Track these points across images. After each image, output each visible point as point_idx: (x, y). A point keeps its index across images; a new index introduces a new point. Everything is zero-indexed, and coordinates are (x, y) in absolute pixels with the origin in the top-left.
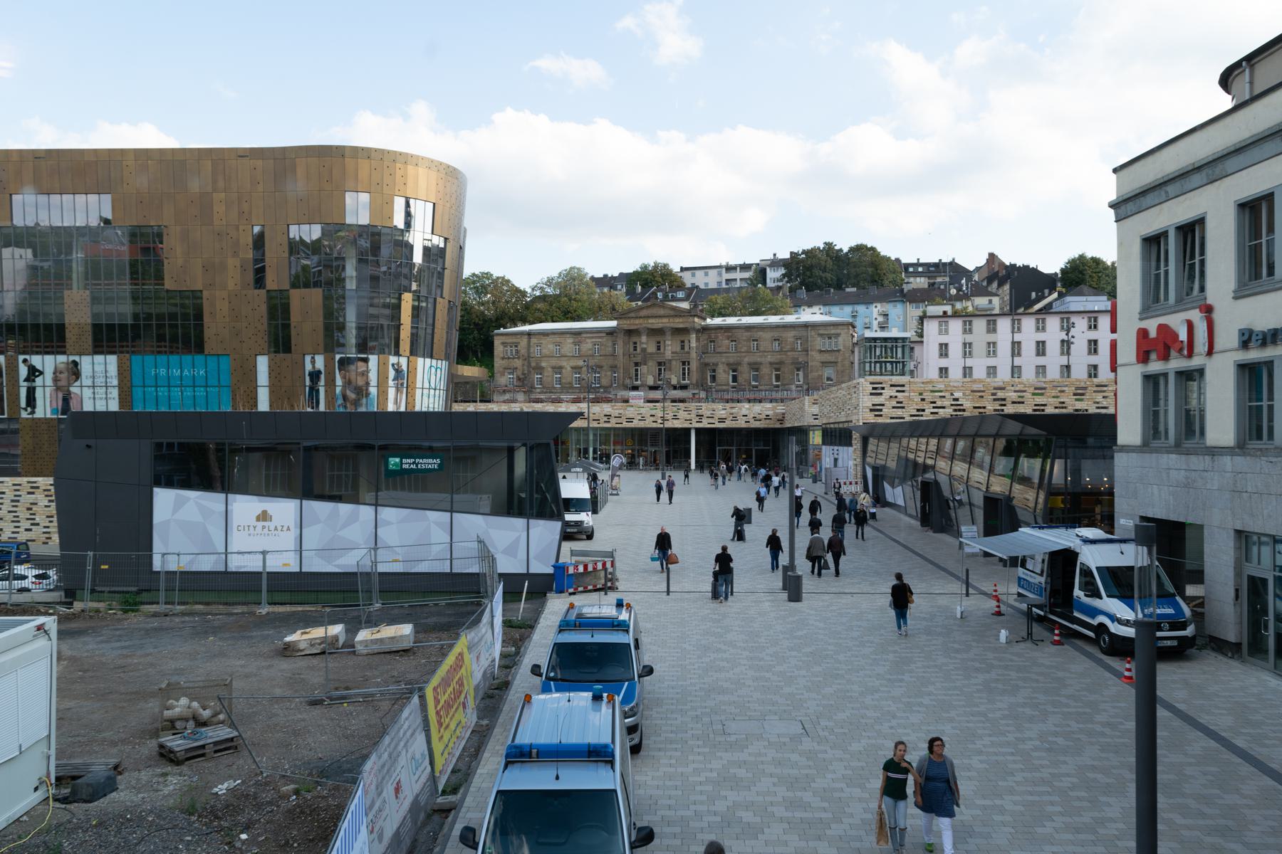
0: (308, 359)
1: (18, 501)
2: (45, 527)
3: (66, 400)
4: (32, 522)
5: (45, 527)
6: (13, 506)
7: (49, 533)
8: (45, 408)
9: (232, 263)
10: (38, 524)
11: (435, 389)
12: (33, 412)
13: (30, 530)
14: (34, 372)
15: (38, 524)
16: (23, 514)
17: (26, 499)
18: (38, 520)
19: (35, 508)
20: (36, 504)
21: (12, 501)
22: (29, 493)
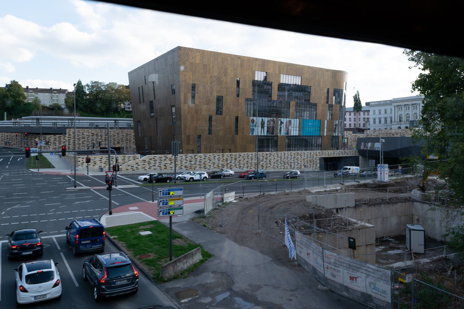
0: (335, 121)
3: (288, 131)
8: (283, 133)
9: (323, 97)
12: (280, 134)
14: (282, 123)
15: (299, 164)
16: (296, 161)
19: (298, 159)
21: (294, 158)
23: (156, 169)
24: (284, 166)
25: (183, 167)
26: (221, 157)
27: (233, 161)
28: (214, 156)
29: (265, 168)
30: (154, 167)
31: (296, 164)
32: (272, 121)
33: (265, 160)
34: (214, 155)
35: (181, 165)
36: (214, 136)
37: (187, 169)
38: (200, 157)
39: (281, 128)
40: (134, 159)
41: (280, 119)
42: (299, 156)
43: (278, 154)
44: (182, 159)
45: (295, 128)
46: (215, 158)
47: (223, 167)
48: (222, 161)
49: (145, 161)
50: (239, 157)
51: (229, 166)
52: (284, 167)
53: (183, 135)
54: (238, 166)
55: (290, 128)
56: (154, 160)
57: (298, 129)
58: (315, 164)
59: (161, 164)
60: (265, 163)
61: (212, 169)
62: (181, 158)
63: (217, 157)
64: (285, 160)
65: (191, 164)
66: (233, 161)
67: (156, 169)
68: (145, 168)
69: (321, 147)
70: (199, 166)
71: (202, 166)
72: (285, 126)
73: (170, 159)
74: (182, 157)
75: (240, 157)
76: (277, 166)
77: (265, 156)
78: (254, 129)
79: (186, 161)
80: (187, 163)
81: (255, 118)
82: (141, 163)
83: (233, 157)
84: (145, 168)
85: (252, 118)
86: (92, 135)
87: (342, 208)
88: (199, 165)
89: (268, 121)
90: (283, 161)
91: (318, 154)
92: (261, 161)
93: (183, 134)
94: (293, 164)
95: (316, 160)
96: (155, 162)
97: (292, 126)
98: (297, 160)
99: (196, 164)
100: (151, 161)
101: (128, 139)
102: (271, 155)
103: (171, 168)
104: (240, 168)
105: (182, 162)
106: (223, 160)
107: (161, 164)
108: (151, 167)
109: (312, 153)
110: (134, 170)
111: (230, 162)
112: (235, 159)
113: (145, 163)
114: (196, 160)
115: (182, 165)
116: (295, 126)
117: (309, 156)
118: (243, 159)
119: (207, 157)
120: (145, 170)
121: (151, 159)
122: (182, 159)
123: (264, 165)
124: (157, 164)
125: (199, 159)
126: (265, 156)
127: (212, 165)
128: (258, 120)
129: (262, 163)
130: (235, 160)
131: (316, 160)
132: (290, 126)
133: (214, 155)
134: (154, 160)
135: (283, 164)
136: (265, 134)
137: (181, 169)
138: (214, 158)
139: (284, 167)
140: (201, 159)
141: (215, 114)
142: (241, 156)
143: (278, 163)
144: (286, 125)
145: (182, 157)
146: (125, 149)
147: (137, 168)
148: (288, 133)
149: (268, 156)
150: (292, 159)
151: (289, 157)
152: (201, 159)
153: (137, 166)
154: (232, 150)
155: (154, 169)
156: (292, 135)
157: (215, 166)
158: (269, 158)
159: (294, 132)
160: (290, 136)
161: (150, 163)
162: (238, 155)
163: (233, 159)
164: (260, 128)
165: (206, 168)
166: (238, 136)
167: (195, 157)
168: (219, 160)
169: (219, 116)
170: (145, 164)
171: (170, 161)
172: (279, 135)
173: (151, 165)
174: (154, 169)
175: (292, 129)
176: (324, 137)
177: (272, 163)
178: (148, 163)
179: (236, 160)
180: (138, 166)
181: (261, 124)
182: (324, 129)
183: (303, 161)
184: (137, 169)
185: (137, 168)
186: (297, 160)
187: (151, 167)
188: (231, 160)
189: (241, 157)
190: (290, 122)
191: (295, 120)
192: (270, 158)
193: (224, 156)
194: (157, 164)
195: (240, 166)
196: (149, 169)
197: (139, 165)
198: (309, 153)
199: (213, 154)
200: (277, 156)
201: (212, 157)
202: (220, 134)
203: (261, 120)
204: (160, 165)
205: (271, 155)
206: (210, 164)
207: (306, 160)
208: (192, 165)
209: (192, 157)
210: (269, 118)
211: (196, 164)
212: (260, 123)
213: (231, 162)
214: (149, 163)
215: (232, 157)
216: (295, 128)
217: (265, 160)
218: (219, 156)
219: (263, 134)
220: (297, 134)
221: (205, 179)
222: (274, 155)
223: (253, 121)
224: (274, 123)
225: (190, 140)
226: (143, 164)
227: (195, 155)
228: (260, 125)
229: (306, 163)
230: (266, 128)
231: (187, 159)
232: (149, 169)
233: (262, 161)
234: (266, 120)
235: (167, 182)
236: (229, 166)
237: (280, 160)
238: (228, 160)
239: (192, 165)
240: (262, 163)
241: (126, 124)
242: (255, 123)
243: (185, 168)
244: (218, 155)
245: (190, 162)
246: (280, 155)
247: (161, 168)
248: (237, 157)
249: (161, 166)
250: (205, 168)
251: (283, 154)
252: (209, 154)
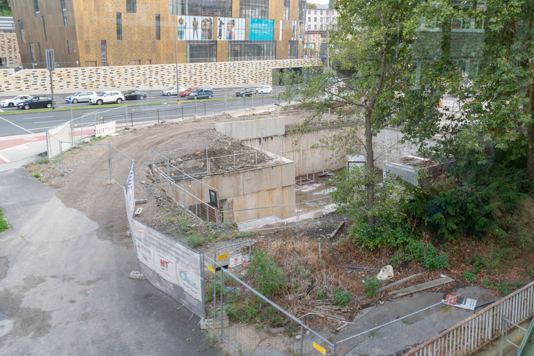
1: (106, 77)
6: (43, 82)
8: (224, 37)
11: (264, 30)
12: (220, 38)
14: (221, 23)
17: (242, 69)
19: (244, 71)
23: (37, 89)
24: (225, 81)
25: (79, 85)
26: (135, 70)
27: (154, 76)
28: (126, 70)
29: (198, 84)
30: (35, 87)
32: (208, 21)
33: (198, 74)
34: (124, 68)
35: (77, 83)
36: (125, 41)
37: (86, 88)
38: (105, 71)
39: (220, 30)
40: (5, 75)
41: (220, 18)
42: (245, 68)
43: (216, 66)
44: (77, 75)
45: (240, 31)
46: (126, 72)
47: (139, 84)
48: (138, 76)
49: (19, 77)
50: (161, 71)
51: (148, 82)
52: (226, 82)
53: (78, 41)
54: (161, 82)
55: (233, 30)
56: (34, 77)
57: (244, 31)
58: (266, 77)
59: (44, 82)
60: (199, 78)
61: (123, 87)
62: (76, 73)
63: (130, 71)
64: (226, 73)
65: (92, 81)
66: (154, 76)
67: (37, 89)
68: (20, 88)
69: (276, 55)
70: (103, 84)
71: (109, 84)
72: (226, 27)
73: (58, 74)
74: (77, 72)
75: (163, 70)
76: (216, 81)
77: (199, 69)
78: (183, 31)
79: (84, 77)
80: (85, 79)
81: (183, 17)
82: (14, 81)
83: (154, 70)
84: (20, 88)
85: (179, 17)
86: (8, 40)
87: (268, 138)
88: (103, 82)
89: (203, 21)
90: (223, 74)
91: (271, 65)
92: (193, 75)
93: (78, 39)
94: (237, 79)
95: (267, 72)
96: (35, 79)
97: (237, 28)
98: (242, 72)
99: (99, 81)
100: (29, 78)
101: (12, 46)
102: (207, 66)
103: (60, 86)
104: (164, 85)
105: (78, 78)
106: (139, 75)
107: (44, 82)
108: (30, 86)
109: (263, 63)
110: (3, 91)
111: (149, 78)
112: (157, 73)
113: (19, 81)
114: (99, 76)
115: (77, 82)
116: (240, 28)
117: (258, 67)
118: (167, 73)
119: (115, 71)
120: (20, 90)
121: (29, 75)
122: (77, 75)
123: (198, 80)
124: (39, 82)
125: (102, 73)
126: (199, 69)
127: (123, 82)
128: (188, 20)
129: (194, 77)
130: (155, 74)
131: (267, 72)
132: (234, 28)
133: (124, 68)
134: (34, 77)
135: (224, 79)
136: (200, 39)
137: (76, 88)
138: (68, 75)
139: (226, 82)
140: (105, 73)
141: (126, 12)
142: (164, 68)
143: (217, 77)
144: (228, 27)
145: (77, 71)
146: (8, 60)
147: (7, 88)
148: (230, 37)
149: (203, 68)
150: (236, 72)
151: (232, 68)
152: (105, 73)
153: (7, 86)
154: (153, 61)
155: (35, 89)
156: (236, 39)
157: (127, 83)
158: (204, 71)
159: (239, 35)
160: (234, 41)
161: (28, 81)
162: (159, 67)
163: (154, 73)
164: (192, 30)
165: (115, 86)
166: (161, 41)
167: (97, 71)
168: (133, 75)
169: (131, 14)
170: (19, 83)
171: (59, 77)
172: (218, 39)
173: (30, 83)
174: (35, 89)
175: (236, 31)
176: (279, 42)
177: (208, 77)
178: (25, 81)
179: (157, 74)
180: (9, 86)
181: (193, 25)
182: (279, 32)
184: (7, 90)
185: (7, 88)
186: (242, 72)
187: (30, 86)
188: (151, 74)
189: (165, 70)
190: (233, 23)
191: (240, 19)
192: (206, 70)
193: (140, 69)
194: (39, 82)
195: (163, 83)
196: (26, 89)
197: (10, 84)
198: (259, 63)
199: (124, 66)
200: (216, 68)
201: (122, 71)
202: (135, 40)
203: (192, 20)
204: (44, 84)
205: (207, 66)
206: (119, 80)
208: (94, 82)
209: (92, 71)
210: (204, 18)
211: (99, 81)
212: (192, 24)
213: (151, 77)
214: (26, 81)
215: (152, 71)
216: (240, 31)
217: (198, 74)
218: (133, 70)
219: (196, 39)
220: (243, 39)
221: (119, 101)
223: (181, 21)
224: (212, 23)
225: (91, 47)
226: (16, 83)
227: (97, 69)
228: (192, 27)
229: (254, 76)
230: (200, 31)
231: (85, 74)
232: (26, 89)
233: (194, 75)
234: (200, 19)
235: (47, 108)
236: (148, 82)
237: (219, 74)
238: (145, 74)
239: (94, 82)
240: (194, 77)
241: (11, 25)
242: (184, 23)
243: (83, 86)
244: (131, 68)
245: (89, 78)
246: (218, 67)
247: (46, 87)
248: (159, 70)
249: (45, 85)
250: (112, 86)
251: (223, 65)
252: (117, 66)
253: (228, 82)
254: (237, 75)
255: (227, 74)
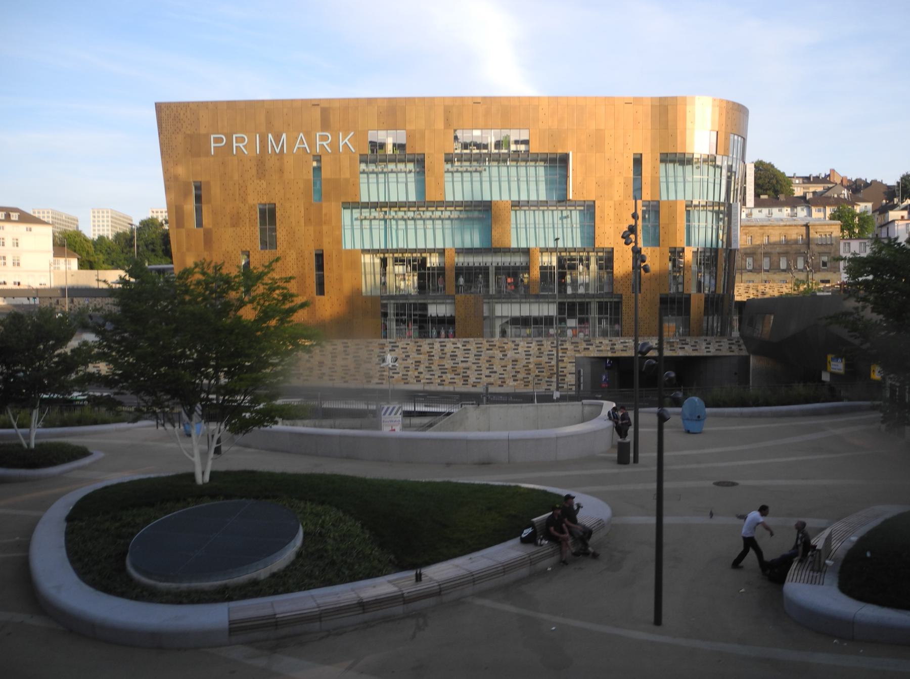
2: (500, 374)
4: (491, 370)
5: (500, 374)
7: (504, 378)
10: (495, 372)
13: (490, 376)
15: (495, 372)
16: (484, 365)
18: (495, 369)
19: (493, 360)
20: (494, 357)
22: (488, 349)
31: (487, 372)
64: (444, 362)
135: (438, 373)
151: (460, 353)
183: (509, 367)
207: (524, 362)
222: (405, 346)
229: (522, 371)
251: (437, 346)
253: (447, 381)
254: (474, 367)
255: (448, 364)
